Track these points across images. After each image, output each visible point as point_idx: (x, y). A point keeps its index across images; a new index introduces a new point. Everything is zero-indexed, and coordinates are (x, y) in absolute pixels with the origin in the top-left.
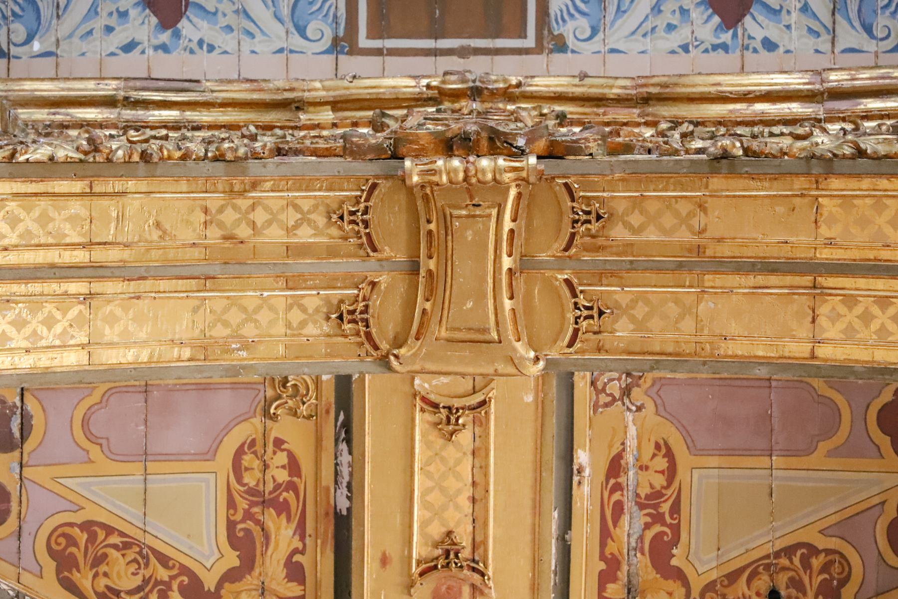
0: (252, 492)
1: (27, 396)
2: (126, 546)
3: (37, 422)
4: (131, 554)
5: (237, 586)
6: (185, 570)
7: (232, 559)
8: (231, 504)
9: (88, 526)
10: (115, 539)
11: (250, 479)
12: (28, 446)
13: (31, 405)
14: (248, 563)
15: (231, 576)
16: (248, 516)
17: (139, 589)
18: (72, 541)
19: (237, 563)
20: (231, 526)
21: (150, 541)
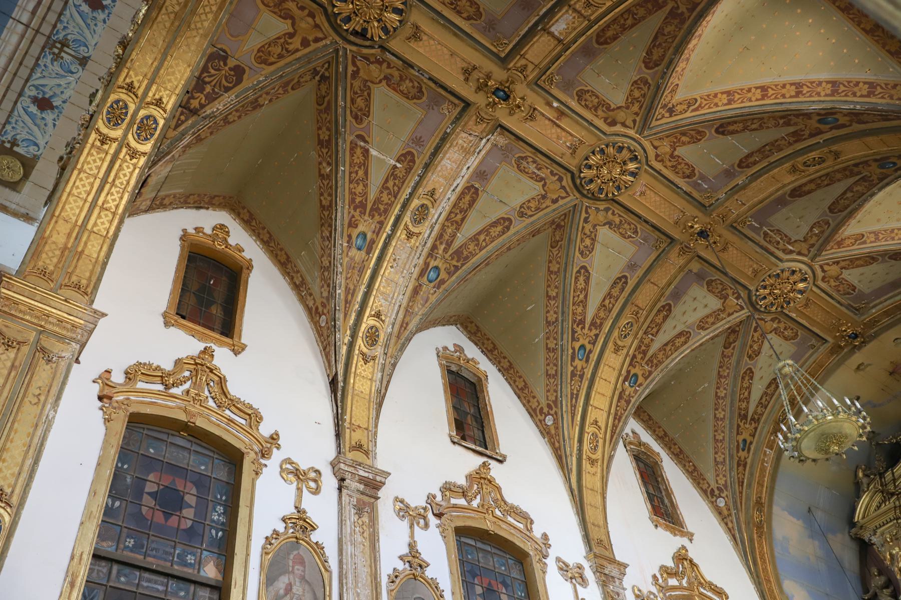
0: (275, 6)
1: (217, 46)
2: (270, 45)
3: (224, 47)
4: (273, 45)
5: (296, 25)
6: (285, 35)
7: (289, 21)
8: (275, 13)
9: (259, 51)
10: (266, 47)
11: (272, 4)
12: (229, 53)
13: (219, 46)
14: (292, 18)
15: (293, 25)
16: (281, 11)
17: (282, 48)
18: (261, 57)
19: (291, 21)
20: (280, 16)
21: (272, 39)
